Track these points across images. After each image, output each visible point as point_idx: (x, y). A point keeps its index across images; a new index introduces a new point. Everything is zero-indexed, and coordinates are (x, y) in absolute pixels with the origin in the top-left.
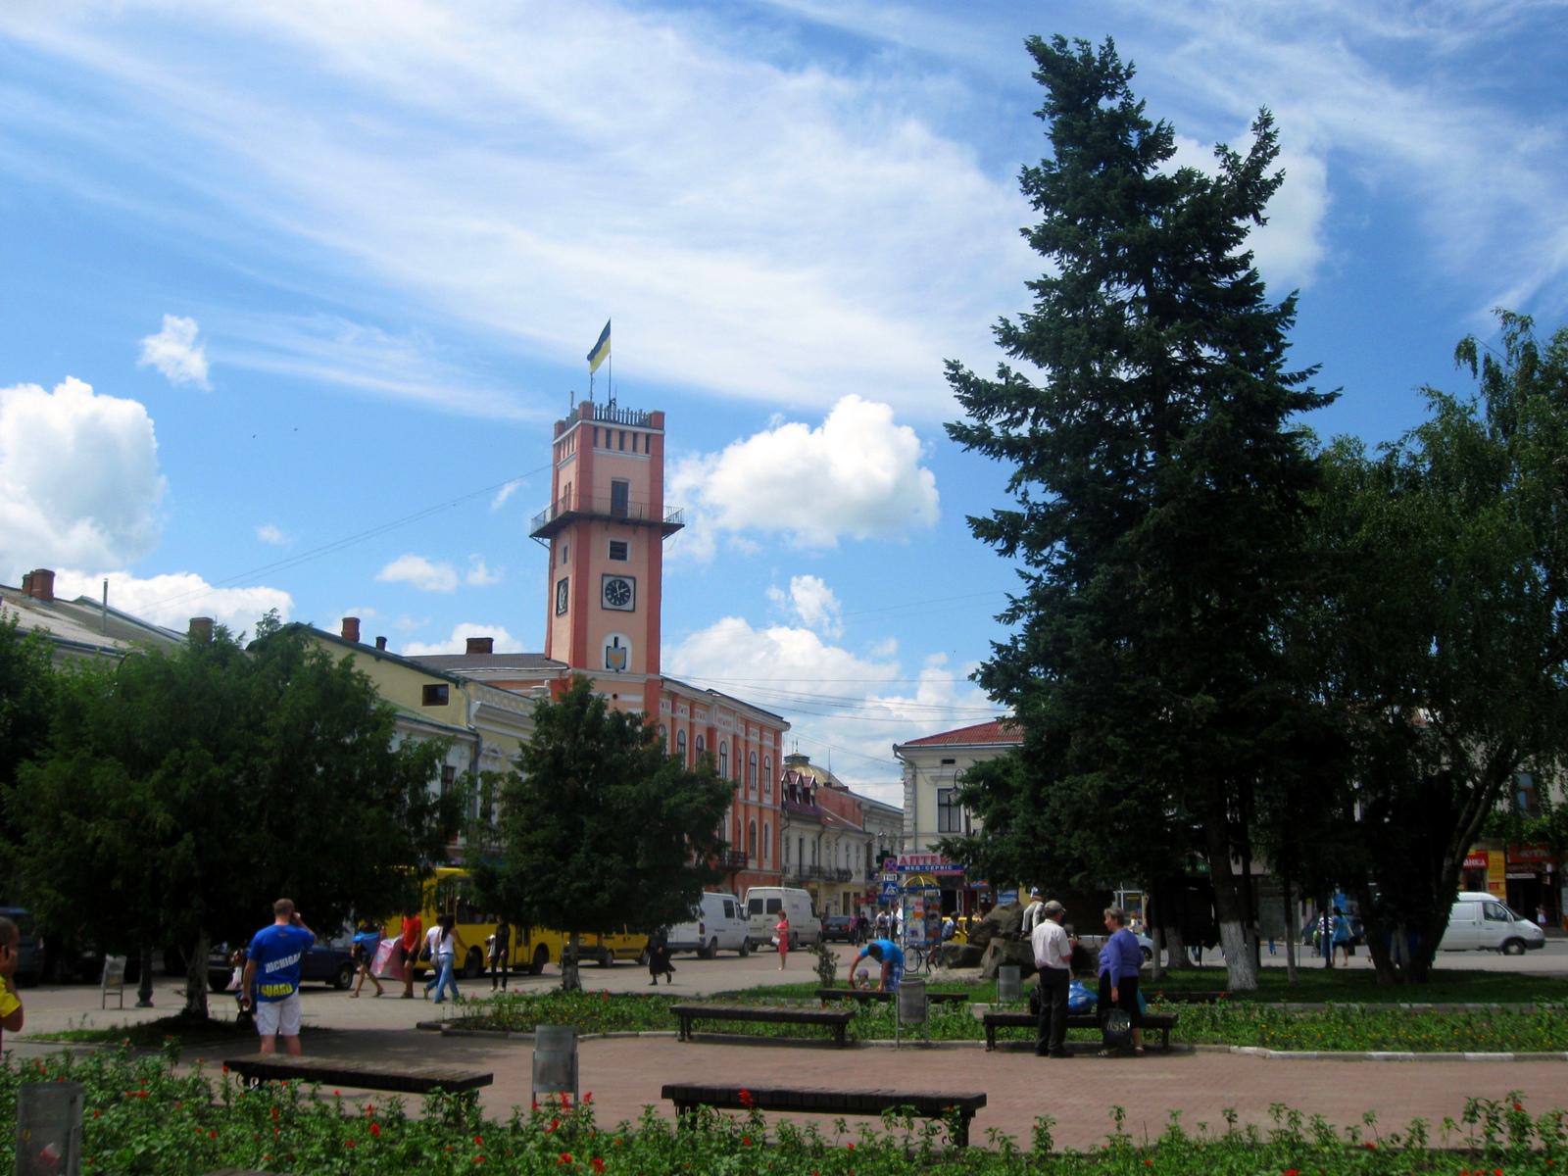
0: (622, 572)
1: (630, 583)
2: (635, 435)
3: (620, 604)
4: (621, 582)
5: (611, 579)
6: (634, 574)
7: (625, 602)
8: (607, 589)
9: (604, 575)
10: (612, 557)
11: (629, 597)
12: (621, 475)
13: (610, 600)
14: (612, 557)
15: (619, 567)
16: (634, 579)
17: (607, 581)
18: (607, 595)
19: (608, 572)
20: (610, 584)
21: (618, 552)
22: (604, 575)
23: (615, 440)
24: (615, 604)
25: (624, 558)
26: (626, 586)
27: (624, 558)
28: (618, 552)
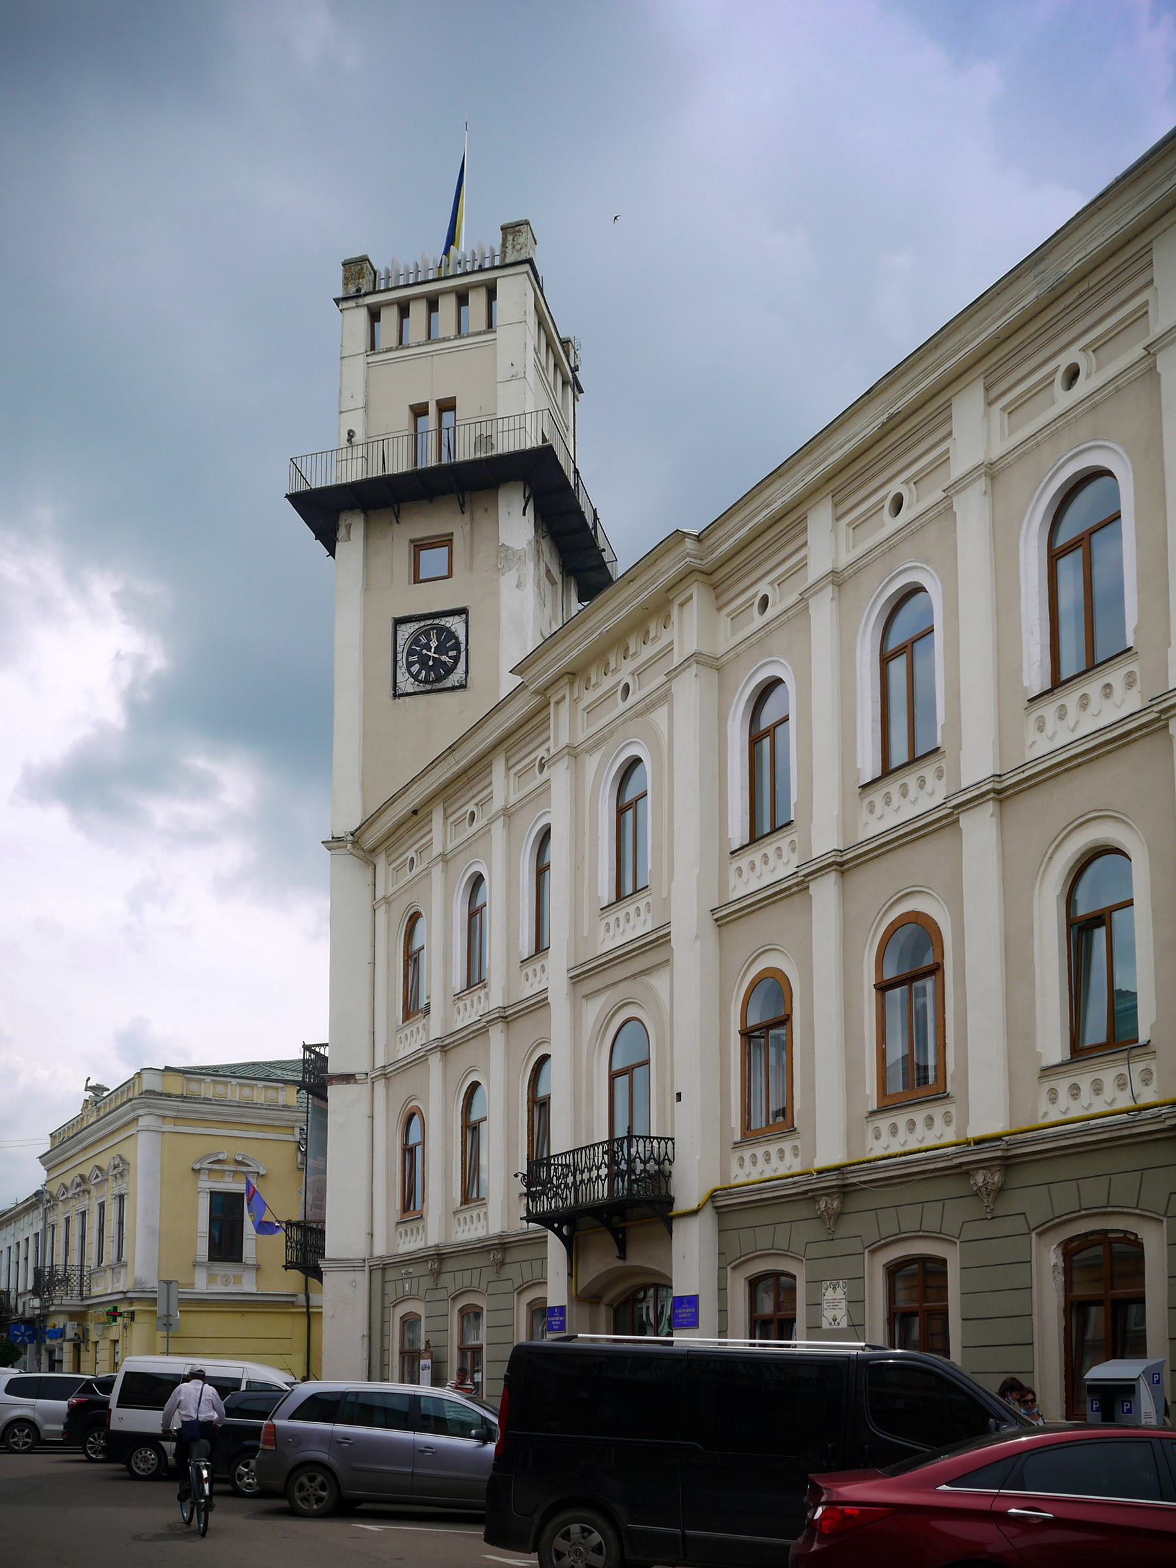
1: (455, 624)
4: (441, 630)
7: (450, 670)
8: (411, 652)
11: (456, 659)
13: (415, 677)
17: (406, 631)
18: (410, 665)
22: (399, 622)
24: (426, 681)
26: (451, 635)
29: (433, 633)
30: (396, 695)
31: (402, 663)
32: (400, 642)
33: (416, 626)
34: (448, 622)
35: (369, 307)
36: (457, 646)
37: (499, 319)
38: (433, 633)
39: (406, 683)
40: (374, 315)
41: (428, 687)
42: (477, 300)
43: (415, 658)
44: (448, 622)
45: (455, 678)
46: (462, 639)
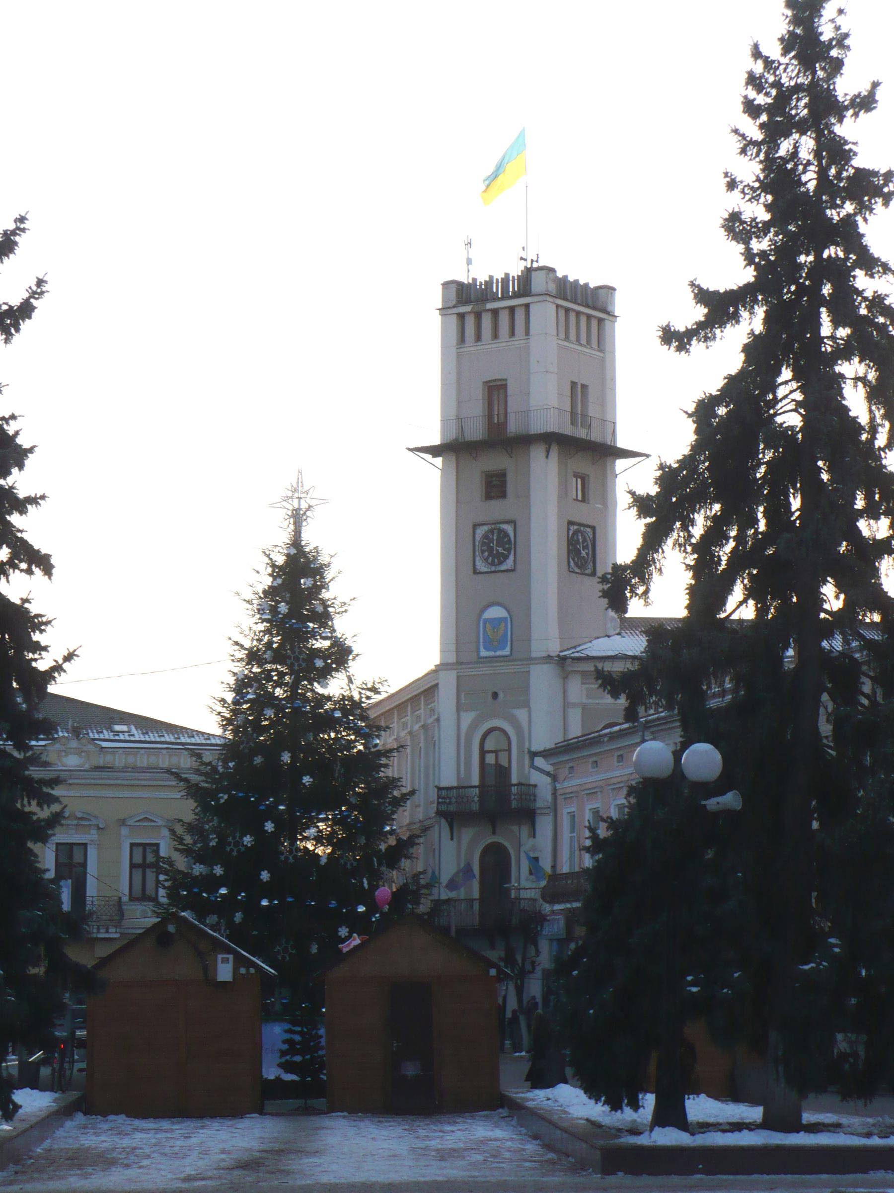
1: (509, 529)
2: (512, 309)
3: (500, 563)
4: (500, 531)
5: (486, 528)
7: (506, 557)
8: (483, 544)
9: (475, 526)
10: (488, 496)
11: (509, 550)
12: (495, 374)
13: (486, 560)
14: (488, 496)
15: (496, 510)
16: (513, 522)
17: (480, 532)
18: (483, 552)
19: (480, 519)
20: (485, 536)
21: (495, 487)
23: (487, 320)
24: (493, 564)
25: (503, 495)
26: (506, 534)
27: (503, 495)
28: (495, 487)
29: (495, 531)
30: (475, 572)
31: (477, 553)
32: (478, 538)
33: (486, 528)
36: (509, 541)
37: (532, 331)
38: (495, 531)
39: (481, 566)
40: (461, 317)
41: (493, 569)
42: (520, 315)
43: (485, 548)
45: (509, 564)
46: (513, 539)
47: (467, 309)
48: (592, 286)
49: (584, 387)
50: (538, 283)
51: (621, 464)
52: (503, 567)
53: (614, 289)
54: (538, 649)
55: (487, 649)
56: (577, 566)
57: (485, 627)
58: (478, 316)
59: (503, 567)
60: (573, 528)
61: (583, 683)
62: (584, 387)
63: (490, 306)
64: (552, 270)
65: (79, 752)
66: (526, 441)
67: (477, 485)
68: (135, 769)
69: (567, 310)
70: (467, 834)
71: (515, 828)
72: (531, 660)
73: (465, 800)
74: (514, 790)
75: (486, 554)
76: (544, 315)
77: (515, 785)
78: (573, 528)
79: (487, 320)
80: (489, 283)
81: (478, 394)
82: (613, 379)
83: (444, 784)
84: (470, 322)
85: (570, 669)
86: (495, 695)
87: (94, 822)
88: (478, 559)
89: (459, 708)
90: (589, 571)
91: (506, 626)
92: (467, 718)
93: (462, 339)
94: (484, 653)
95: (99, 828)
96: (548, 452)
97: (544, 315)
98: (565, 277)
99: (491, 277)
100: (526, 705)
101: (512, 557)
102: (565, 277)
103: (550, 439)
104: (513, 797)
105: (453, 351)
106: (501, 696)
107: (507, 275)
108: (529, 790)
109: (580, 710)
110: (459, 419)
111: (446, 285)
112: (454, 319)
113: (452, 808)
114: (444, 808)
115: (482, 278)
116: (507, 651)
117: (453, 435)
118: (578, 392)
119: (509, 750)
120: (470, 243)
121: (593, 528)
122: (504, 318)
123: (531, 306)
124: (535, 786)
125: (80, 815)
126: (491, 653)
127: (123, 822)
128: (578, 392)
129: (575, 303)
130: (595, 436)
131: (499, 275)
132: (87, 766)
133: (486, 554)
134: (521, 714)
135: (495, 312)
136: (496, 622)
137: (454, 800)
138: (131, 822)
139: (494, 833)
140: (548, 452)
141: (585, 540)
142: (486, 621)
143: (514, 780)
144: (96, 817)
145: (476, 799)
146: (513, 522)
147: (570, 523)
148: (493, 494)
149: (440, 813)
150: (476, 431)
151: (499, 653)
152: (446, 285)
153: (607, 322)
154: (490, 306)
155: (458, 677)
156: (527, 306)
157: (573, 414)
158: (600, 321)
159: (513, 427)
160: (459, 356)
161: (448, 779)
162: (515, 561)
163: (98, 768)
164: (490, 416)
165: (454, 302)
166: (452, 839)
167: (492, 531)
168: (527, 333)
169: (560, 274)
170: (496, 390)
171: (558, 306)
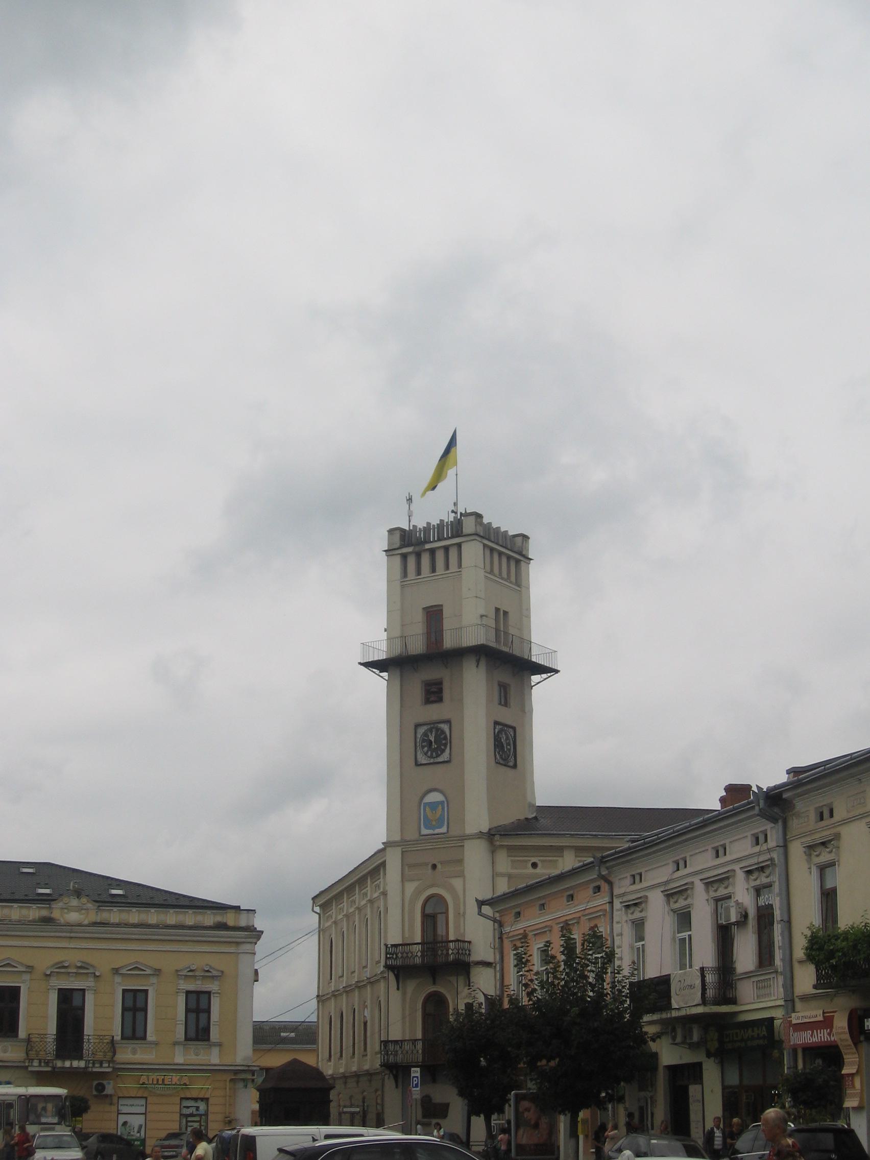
0: (435, 718)
1: (445, 727)
2: (446, 549)
3: (438, 756)
4: (438, 729)
5: (426, 728)
6: (445, 717)
7: (443, 751)
8: (424, 741)
9: (417, 726)
11: (445, 745)
13: (426, 754)
15: (434, 712)
17: (421, 731)
18: (423, 747)
19: (421, 721)
20: (425, 734)
21: (434, 693)
22: (417, 726)
23: (425, 559)
24: (431, 757)
25: (440, 700)
26: (443, 732)
27: (440, 700)
28: (434, 693)
30: (417, 764)
32: (419, 736)
33: (426, 728)
34: (442, 726)
35: (401, 554)
36: (445, 738)
39: (422, 759)
40: (404, 557)
41: (432, 761)
42: (453, 553)
44: (442, 726)
45: (445, 756)
47: (410, 549)
48: (511, 533)
49: (505, 613)
50: (469, 526)
51: (535, 678)
52: (440, 759)
53: (525, 538)
54: (470, 829)
55: (427, 827)
56: (502, 758)
57: (425, 810)
58: (418, 555)
59: (440, 759)
60: (498, 728)
61: (509, 856)
62: (505, 613)
63: (427, 546)
64: (479, 516)
65: (79, 909)
66: (459, 654)
67: (417, 691)
68: (127, 925)
69: (492, 550)
70: (411, 986)
71: (453, 979)
72: (464, 838)
73: (410, 955)
74: (451, 945)
75: (426, 749)
76: (473, 552)
77: (452, 941)
78: (498, 728)
79: (425, 559)
80: (427, 529)
81: (419, 617)
82: (528, 609)
83: (391, 942)
84: (411, 561)
85: (498, 843)
86: (434, 867)
87: (91, 971)
88: (419, 753)
89: (404, 879)
90: (511, 764)
91: (443, 809)
92: (411, 887)
93: (405, 573)
94: (424, 831)
95: (96, 977)
96: (478, 662)
97: (473, 552)
98: (490, 524)
99: (428, 524)
100: (461, 875)
101: (448, 751)
102: (490, 524)
103: (481, 652)
104: (450, 952)
105: (397, 585)
106: (439, 866)
107: (442, 521)
108: (464, 944)
109: (506, 879)
110: (403, 637)
111: (391, 531)
112: (397, 560)
113: (399, 962)
114: (389, 962)
115: (421, 525)
116: (444, 830)
117: (397, 651)
118: (501, 615)
119: (446, 913)
120: (410, 500)
121: (514, 729)
122: (440, 556)
123: (464, 547)
124: (470, 942)
125: (79, 964)
126: (430, 832)
127: (116, 971)
128: (501, 615)
129: (497, 544)
130: (517, 652)
131: (435, 522)
132: (86, 922)
133: (426, 749)
134: (457, 883)
135: (432, 552)
136: (433, 806)
137: (400, 955)
138: (124, 971)
139: (434, 983)
140: (478, 662)
141: (507, 738)
142: (426, 804)
143: (451, 938)
144: (93, 966)
145: (419, 954)
146: (448, 722)
147: (496, 723)
148: (432, 699)
149: (388, 967)
150: (417, 646)
151: (437, 831)
152: (391, 531)
153: (523, 564)
154: (427, 546)
155: (403, 852)
156: (459, 545)
157: (497, 630)
158: (518, 562)
159: (449, 642)
160: (403, 587)
161: (394, 937)
162: (450, 754)
163: (95, 924)
164: (428, 634)
165: (398, 545)
166: (398, 989)
167: (431, 730)
168: (460, 566)
169: (485, 521)
170: (434, 615)
171: (485, 546)
